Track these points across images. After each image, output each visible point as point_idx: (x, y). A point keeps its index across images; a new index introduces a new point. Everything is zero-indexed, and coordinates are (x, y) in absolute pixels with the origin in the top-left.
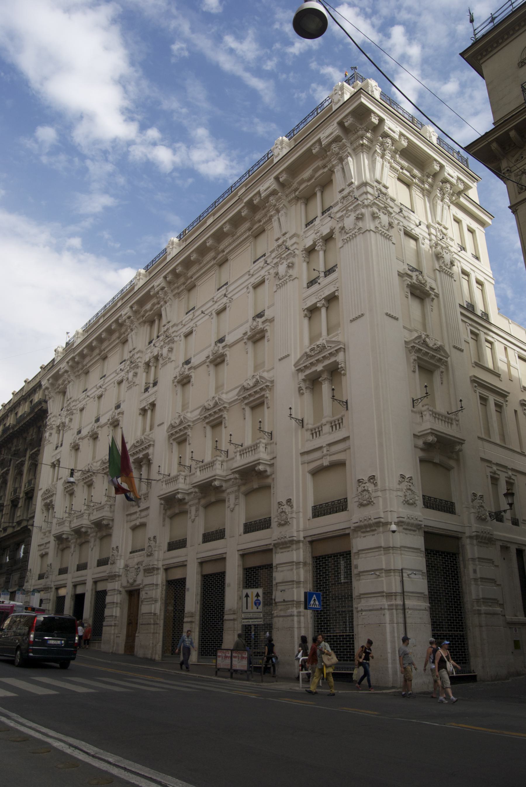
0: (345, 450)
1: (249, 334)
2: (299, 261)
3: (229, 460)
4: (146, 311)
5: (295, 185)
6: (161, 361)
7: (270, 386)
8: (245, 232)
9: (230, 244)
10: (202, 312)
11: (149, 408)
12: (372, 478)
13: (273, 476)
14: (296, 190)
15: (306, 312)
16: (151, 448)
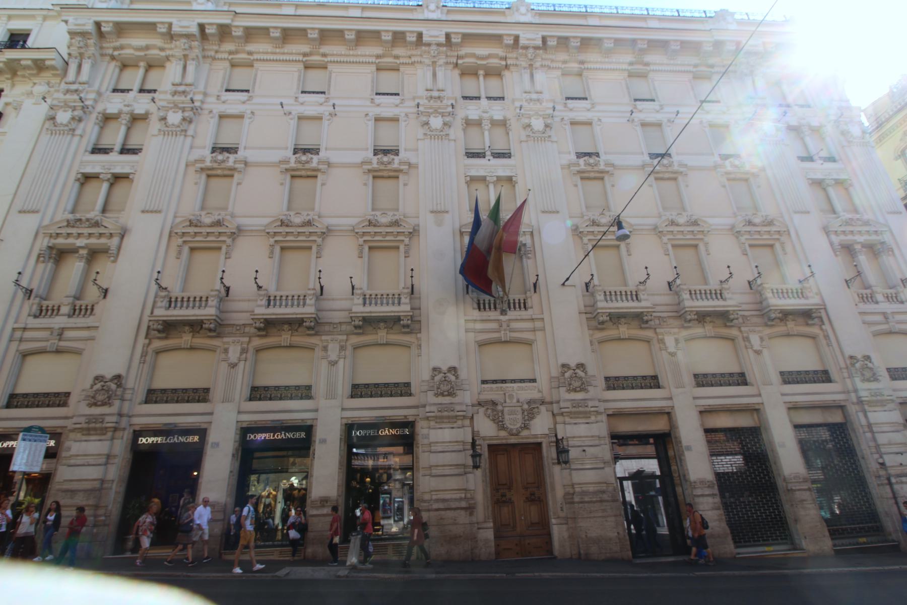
0: (534, 330)
1: (375, 166)
2: (458, 123)
3: (324, 299)
4: (130, 46)
5: (464, 51)
6: (155, 125)
7: (414, 233)
8: (370, 56)
9: (341, 55)
10: (282, 104)
11: (108, 180)
12: (581, 366)
13: (419, 335)
14: (462, 57)
15: (468, 179)
16: (115, 241)
